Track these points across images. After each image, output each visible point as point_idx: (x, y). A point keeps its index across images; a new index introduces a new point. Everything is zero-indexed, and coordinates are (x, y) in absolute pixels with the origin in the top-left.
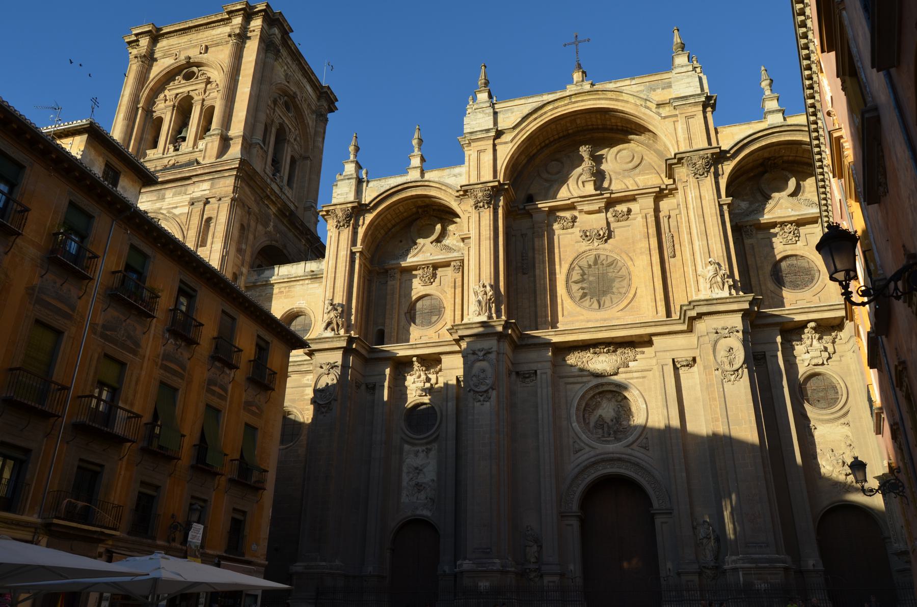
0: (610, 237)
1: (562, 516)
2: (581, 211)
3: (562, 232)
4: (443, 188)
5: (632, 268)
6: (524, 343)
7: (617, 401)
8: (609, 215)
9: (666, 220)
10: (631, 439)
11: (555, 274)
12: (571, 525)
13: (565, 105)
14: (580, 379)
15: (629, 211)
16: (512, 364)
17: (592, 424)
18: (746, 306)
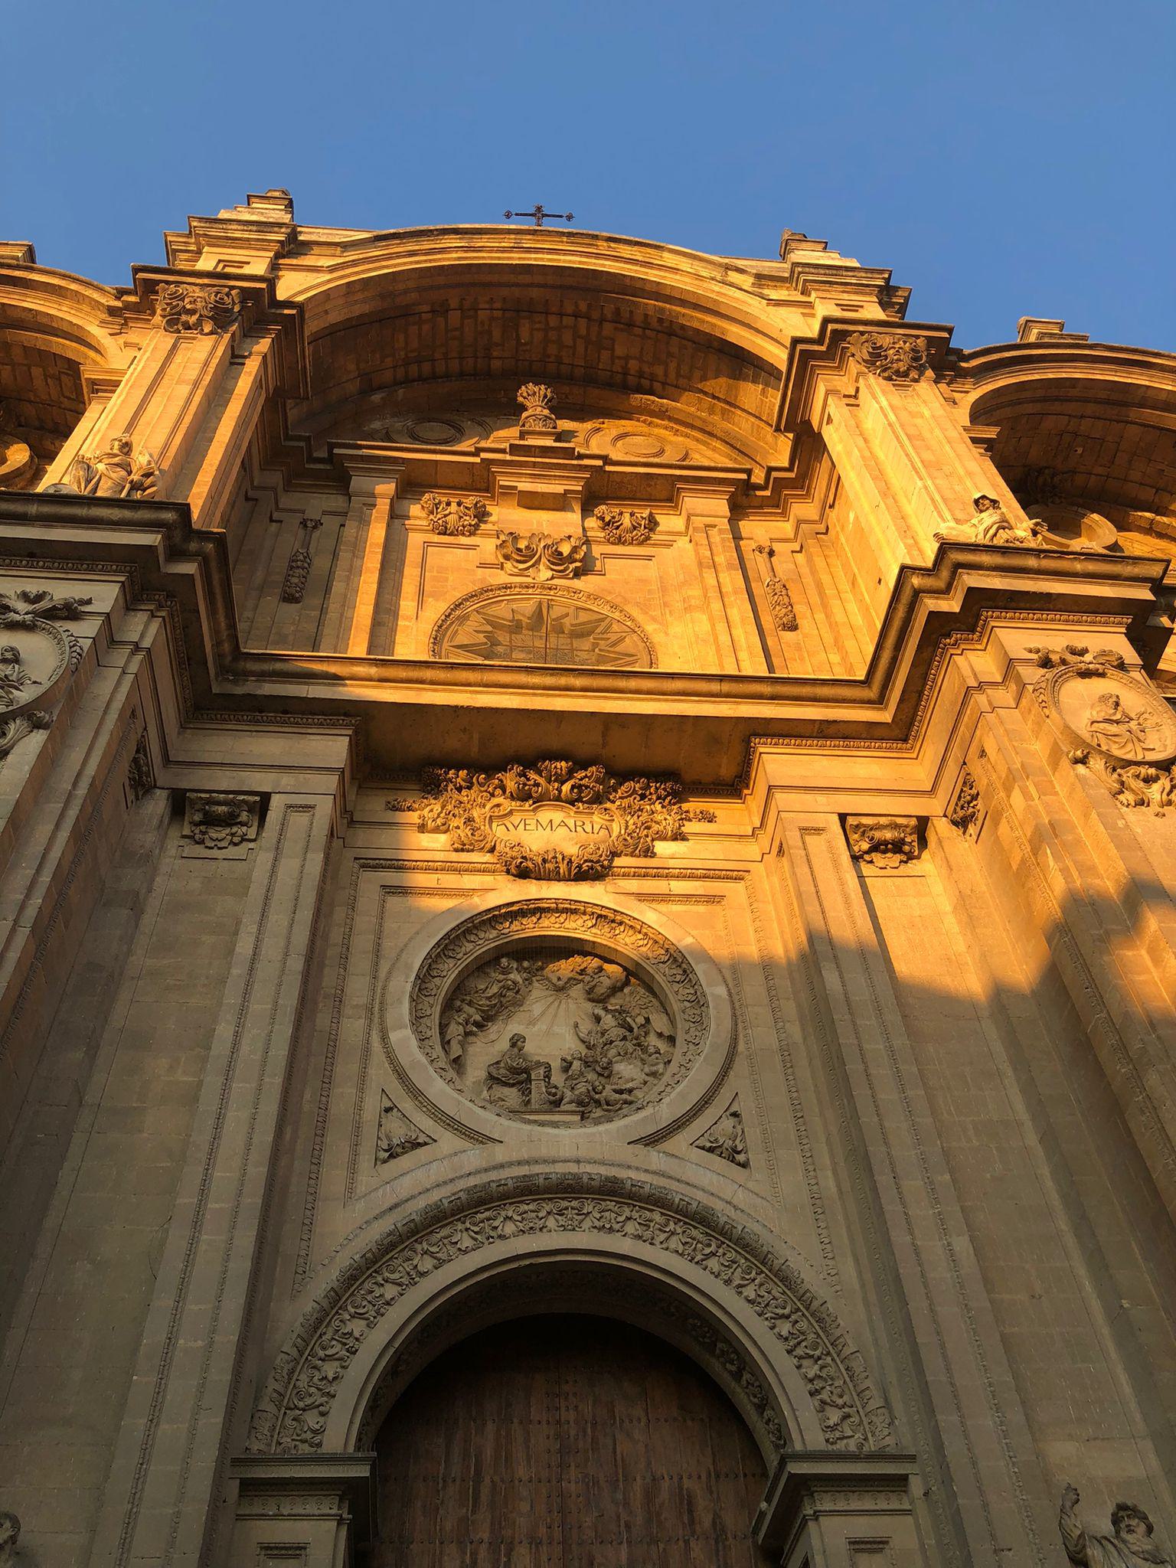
0: (584, 569)
1: (251, 1488)
2: (509, 492)
3: (436, 538)
4: (73, 286)
5: (657, 638)
6: (239, 690)
7: (592, 996)
8: (592, 523)
9: (762, 559)
10: (666, 1112)
11: (395, 614)
12: (296, 1551)
13: (504, 250)
14: (450, 880)
15: (652, 524)
16: (167, 761)
17: (476, 1071)
18: (1145, 594)
